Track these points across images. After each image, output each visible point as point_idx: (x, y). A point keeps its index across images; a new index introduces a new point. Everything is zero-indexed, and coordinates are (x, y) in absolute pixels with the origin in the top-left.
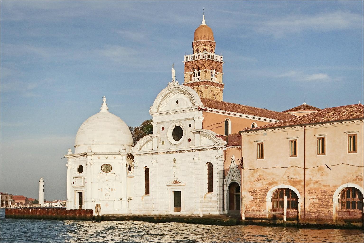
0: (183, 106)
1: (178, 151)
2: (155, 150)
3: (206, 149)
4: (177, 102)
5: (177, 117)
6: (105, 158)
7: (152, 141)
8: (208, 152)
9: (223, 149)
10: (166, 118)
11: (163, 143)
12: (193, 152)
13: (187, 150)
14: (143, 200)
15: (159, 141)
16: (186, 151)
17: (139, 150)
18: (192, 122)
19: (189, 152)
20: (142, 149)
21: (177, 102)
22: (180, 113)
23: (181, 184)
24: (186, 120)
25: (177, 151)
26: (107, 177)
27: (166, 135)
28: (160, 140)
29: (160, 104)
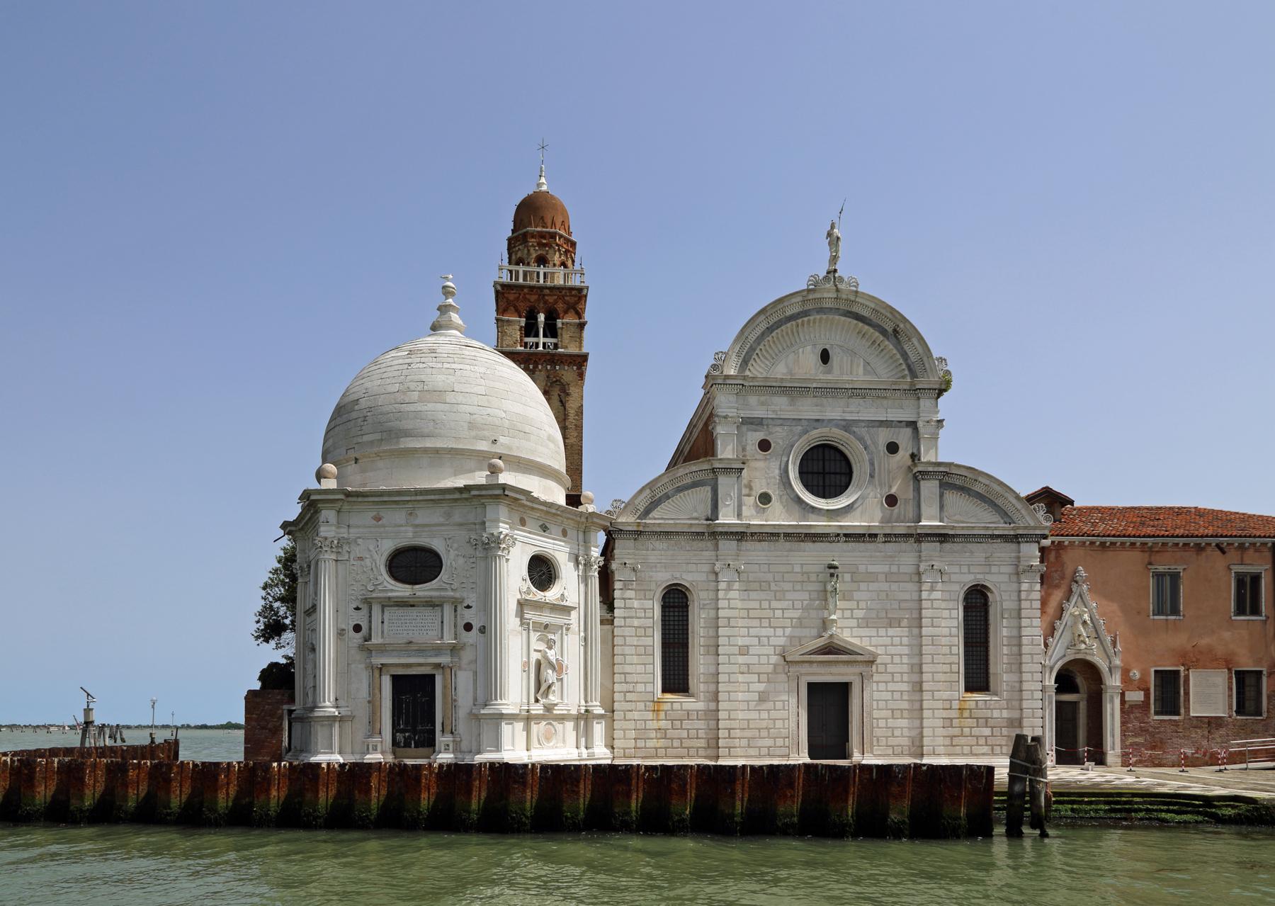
0: (851, 374)
1: (845, 535)
2: (727, 518)
3: (968, 538)
4: (825, 357)
5: (835, 411)
6: (541, 526)
7: (709, 488)
8: (979, 552)
9: (1039, 543)
10: (781, 406)
11: (765, 498)
12: (910, 545)
13: (885, 535)
14: (662, 715)
15: (745, 491)
16: (881, 539)
17: (638, 518)
18: (903, 438)
19: (889, 542)
20: (655, 514)
21: (825, 357)
22: (851, 397)
23: (859, 658)
24: (873, 427)
25: (838, 535)
26: (546, 618)
27: (777, 472)
28: (751, 488)
29: (752, 349)
